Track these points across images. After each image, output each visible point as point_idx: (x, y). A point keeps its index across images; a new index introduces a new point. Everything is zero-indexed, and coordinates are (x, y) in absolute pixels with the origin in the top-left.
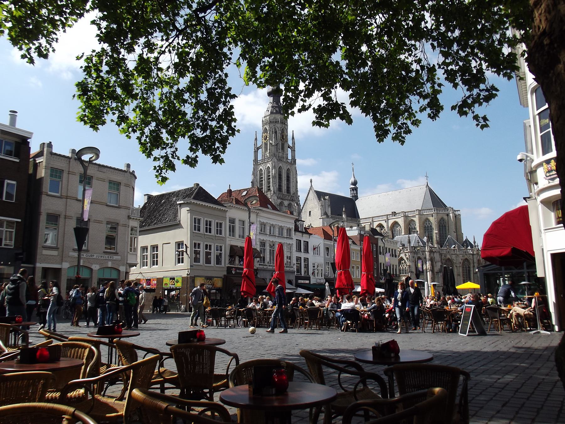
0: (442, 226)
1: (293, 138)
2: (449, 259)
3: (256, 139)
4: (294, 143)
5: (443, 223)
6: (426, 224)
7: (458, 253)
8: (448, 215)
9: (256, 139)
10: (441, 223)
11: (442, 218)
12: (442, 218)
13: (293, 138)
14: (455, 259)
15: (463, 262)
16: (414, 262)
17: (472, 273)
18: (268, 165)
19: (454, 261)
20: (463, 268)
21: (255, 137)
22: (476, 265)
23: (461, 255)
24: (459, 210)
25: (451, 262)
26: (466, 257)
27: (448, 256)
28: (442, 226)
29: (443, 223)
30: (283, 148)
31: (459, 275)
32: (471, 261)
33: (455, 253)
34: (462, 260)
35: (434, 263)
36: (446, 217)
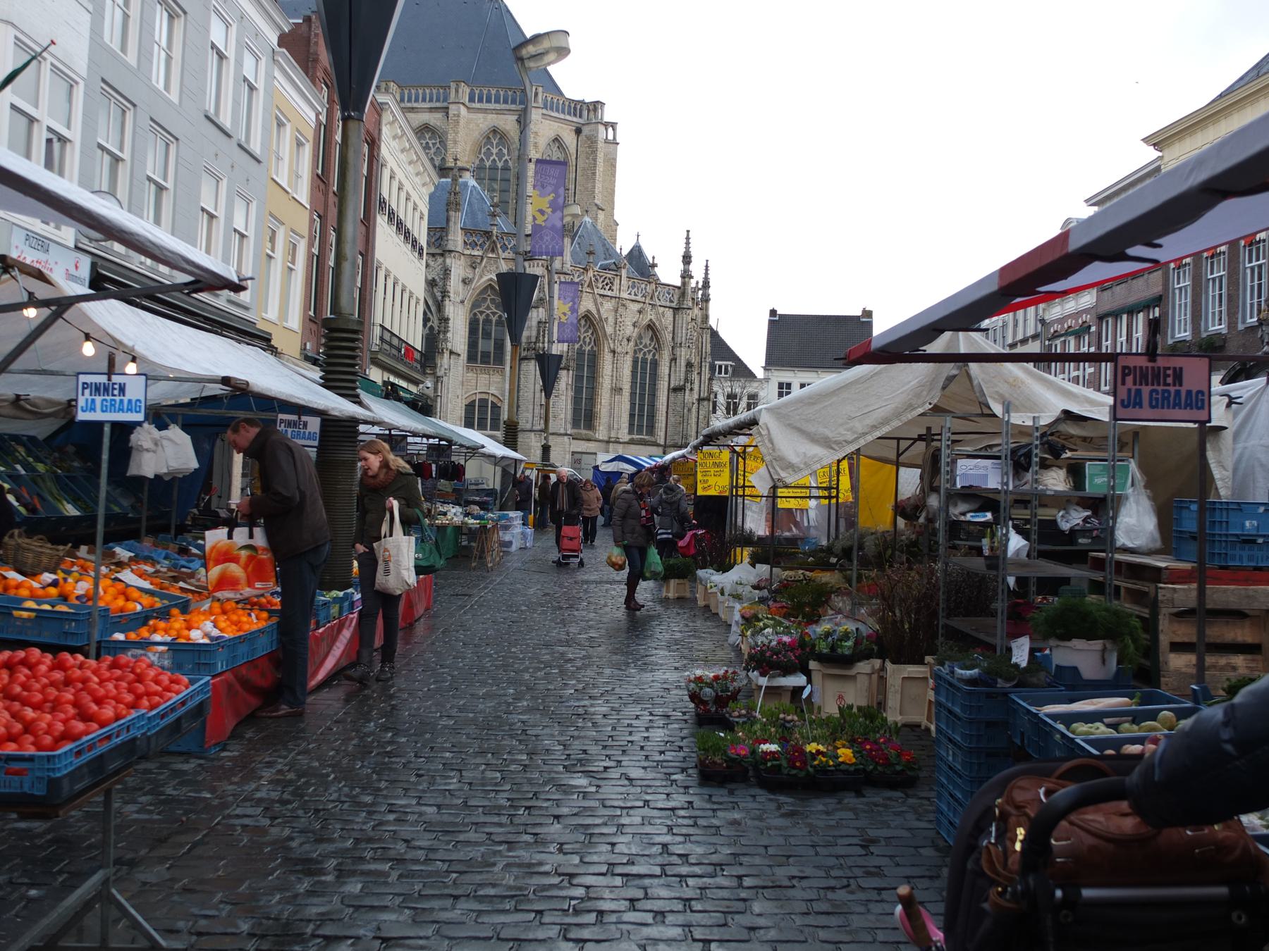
2: (587, 317)
6: (488, 153)
7: (624, 295)
11: (557, 140)
12: (557, 140)
15: (640, 337)
16: (468, 304)
17: (663, 387)
19: (609, 330)
20: (635, 362)
23: (635, 307)
24: (613, 125)
25: (595, 331)
26: (650, 315)
27: (587, 304)
31: (617, 390)
34: (634, 325)
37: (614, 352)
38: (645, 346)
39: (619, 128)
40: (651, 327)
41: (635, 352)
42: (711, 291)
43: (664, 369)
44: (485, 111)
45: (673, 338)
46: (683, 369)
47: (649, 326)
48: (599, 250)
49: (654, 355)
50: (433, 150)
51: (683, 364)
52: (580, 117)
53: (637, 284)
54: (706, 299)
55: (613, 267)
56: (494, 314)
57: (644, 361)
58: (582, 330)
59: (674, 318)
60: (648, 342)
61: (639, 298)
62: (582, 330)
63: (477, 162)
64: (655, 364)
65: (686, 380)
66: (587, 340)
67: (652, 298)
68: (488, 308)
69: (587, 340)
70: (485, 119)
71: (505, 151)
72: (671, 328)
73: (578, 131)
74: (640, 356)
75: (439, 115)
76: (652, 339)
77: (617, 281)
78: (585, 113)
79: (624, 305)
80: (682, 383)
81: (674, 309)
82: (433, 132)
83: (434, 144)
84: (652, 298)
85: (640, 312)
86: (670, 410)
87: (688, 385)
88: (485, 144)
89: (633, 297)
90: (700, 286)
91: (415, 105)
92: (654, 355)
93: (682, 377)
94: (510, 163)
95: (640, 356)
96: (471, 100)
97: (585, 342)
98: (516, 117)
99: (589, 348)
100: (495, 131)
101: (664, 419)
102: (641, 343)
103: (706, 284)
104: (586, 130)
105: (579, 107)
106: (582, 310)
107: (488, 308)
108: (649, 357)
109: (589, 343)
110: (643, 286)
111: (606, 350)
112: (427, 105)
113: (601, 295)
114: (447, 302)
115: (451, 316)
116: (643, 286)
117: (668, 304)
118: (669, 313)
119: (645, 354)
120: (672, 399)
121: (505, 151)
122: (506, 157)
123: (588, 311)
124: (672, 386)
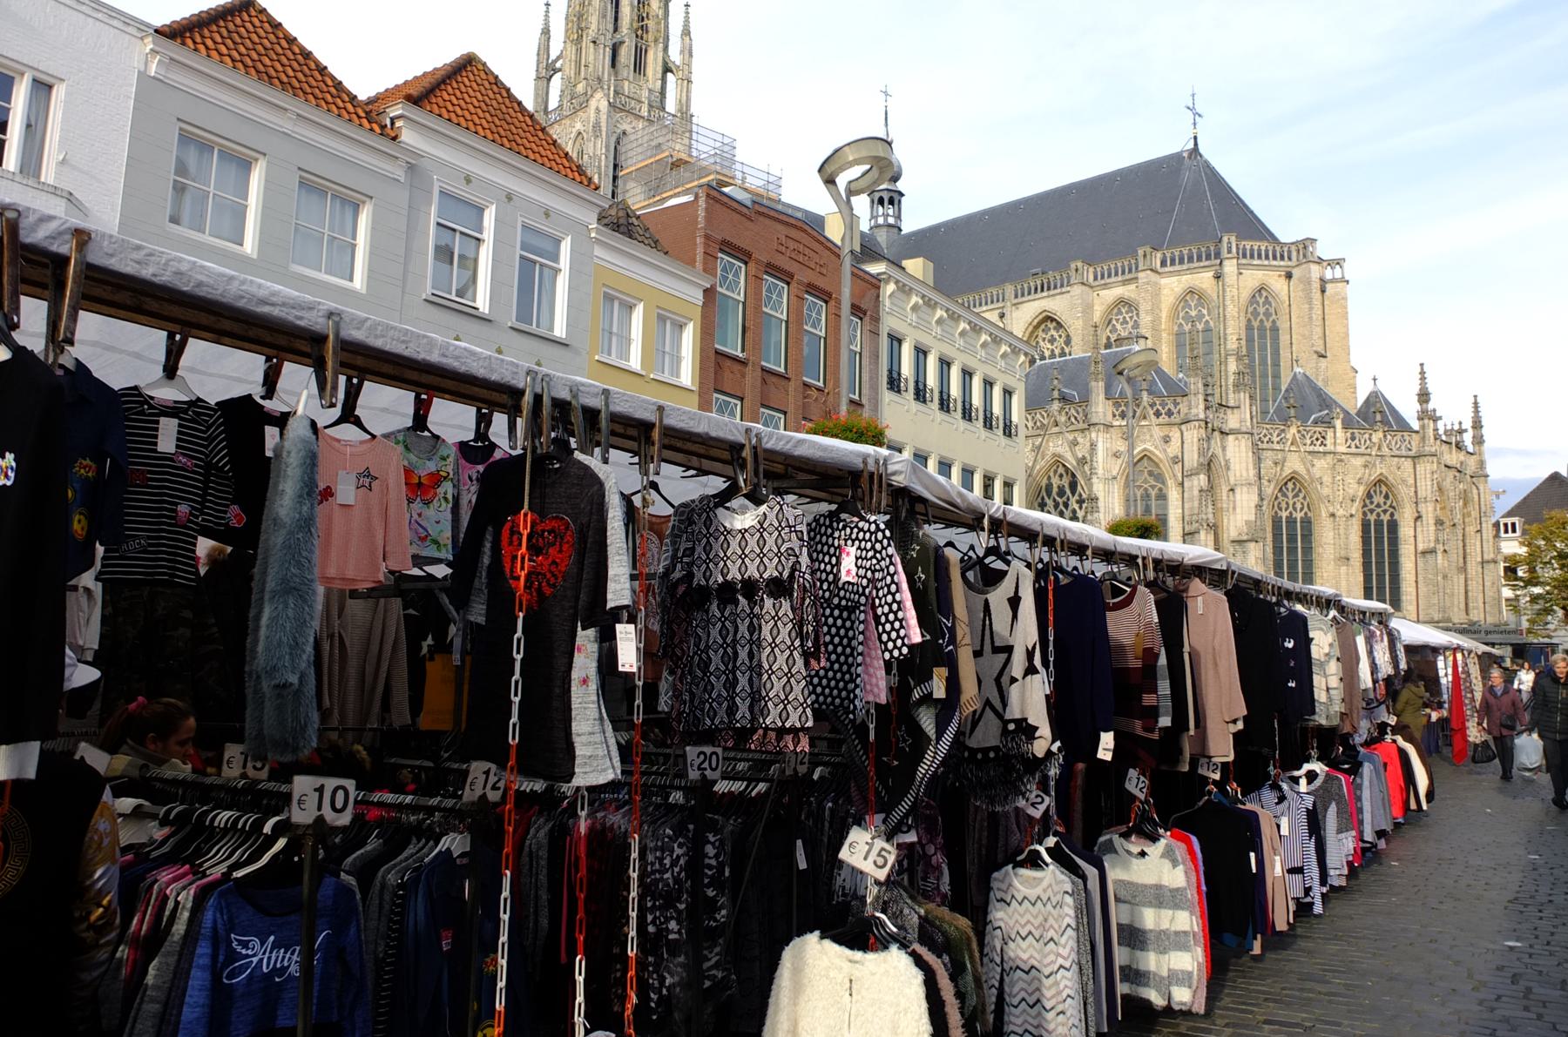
0: (1262, 329)
1: (686, 32)
3: (546, 32)
4: (688, 52)
5: (1268, 314)
7: (1342, 449)
8: (1289, 276)
9: (546, 32)
10: (1255, 313)
13: (686, 32)
14: (1327, 479)
15: (1369, 496)
18: (579, 126)
21: (540, 26)
22: (1429, 511)
23: (1359, 461)
26: (1380, 469)
27: (1294, 464)
28: (1262, 329)
29: (1268, 314)
30: (639, 66)
32: (1405, 493)
33: (1330, 447)
34: (1359, 482)
35: (1225, 489)
36: (1278, 284)
37: (1333, 515)
38: (1378, 506)
39: (1345, 265)
40: (1380, 482)
41: (1365, 514)
42: (1486, 432)
43: (1406, 531)
44: (1178, 273)
45: (1416, 492)
46: (1432, 528)
47: (1380, 481)
48: (1313, 400)
49: (1392, 515)
50: (1130, 325)
51: (1432, 522)
52: (1290, 259)
53: (1357, 435)
54: (1478, 440)
55: (1327, 419)
56: (1153, 487)
57: (1379, 523)
58: (1290, 495)
59: (1415, 468)
60: (1382, 500)
61: (1362, 450)
62: (1290, 495)
63: (1176, 328)
64: (1393, 526)
65: (1437, 541)
66: (1299, 506)
67: (1379, 449)
68: (1145, 481)
69: (1299, 506)
70: (1179, 282)
71: (1205, 312)
72: (1411, 481)
73: (1289, 276)
74: (1372, 518)
75: (1133, 287)
76: (1387, 497)
77: (1330, 434)
78: (1294, 254)
79: (1341, 461)
80: (1432, 545)
81: (1413, 458)
82: (1130, 306)
83: (1131, 318)
84: (1379, 449)
85: (1366, 466)
86: (1420, 578)
87: (1440, 547)
88: (1183, 308)
89: (1353, 450)
90: (1468, 424)
91: (1108, 281)
92: (1392, 515)
93: (1432, 538)
94: (1212, 324)
95: (1372, 518)
96: (1163, 264)
97: (1295, 509)
98: (1212, 274)
99: (1302, 514)
100: (1191, 292)
101: (1412, 590)
102: (1372, 503)
103: (1477, 425)
104: (1296, 273)
105: (1286, 249)
106: (1287, 472)
107: (1145, 481)
108: (1385, 518)
109: (1302, 509)
110: (1367, 436)
111: (1324, 514)
112: (1120, 278)
113: (1310, 452)
114: (1095, 480)
115: (1101, 495)
116: (1367, 436)
117: (1404, 453)
118: (1408, 464)
119: (1378, 515)
120: (1420, 564)
121: (1205, 312)
122: (1207, 318)
123: (1294, 472)
124: (1421, 547)
